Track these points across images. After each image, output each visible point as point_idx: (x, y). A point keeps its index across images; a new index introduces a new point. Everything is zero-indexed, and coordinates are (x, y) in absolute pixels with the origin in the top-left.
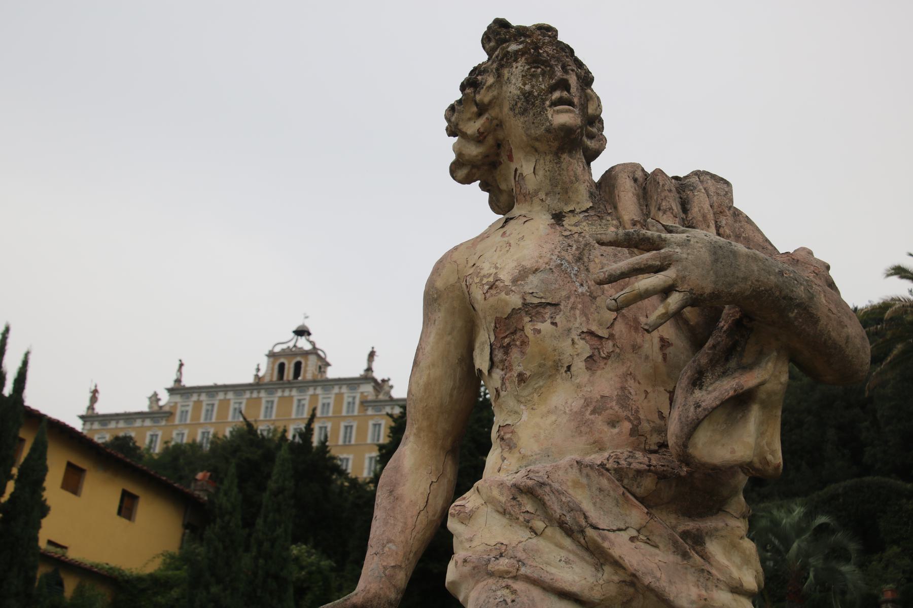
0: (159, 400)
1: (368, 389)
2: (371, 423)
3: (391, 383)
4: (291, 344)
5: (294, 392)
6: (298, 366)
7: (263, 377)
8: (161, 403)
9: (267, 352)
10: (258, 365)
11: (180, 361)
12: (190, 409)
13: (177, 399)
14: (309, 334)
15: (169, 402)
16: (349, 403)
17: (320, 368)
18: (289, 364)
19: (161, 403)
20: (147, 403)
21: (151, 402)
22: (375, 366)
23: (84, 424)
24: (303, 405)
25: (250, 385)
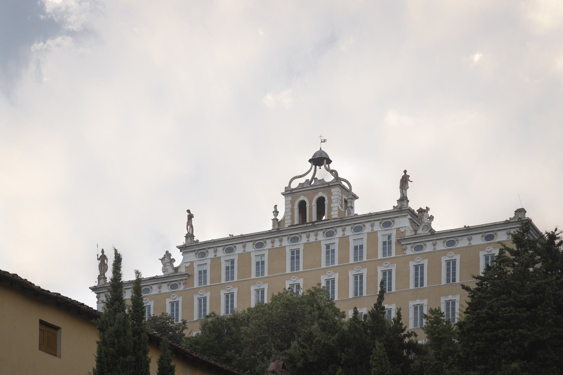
0: (173, 260)
1: (404, 223)
2: (412, 264)
3: (430, 213)
4: (309, 177)
5: (321, 236)
6: (321, 202)
7: (283, 220)
8: (176, 265)
9: (283, 191)
10: (276, 206)
11: (188, 211)
12: (208, 268)
13: (192, 257)
14: (329, 161)
15: (183, 262)
16: (384, 243)
17: (346, 202)
18: (311, 202)
19: (176, 265)
20: (161, 265)
21: (164, 265)
22: (410, 194)
23: (98, 297)
24: (333, 251)
25: (270, 232)
